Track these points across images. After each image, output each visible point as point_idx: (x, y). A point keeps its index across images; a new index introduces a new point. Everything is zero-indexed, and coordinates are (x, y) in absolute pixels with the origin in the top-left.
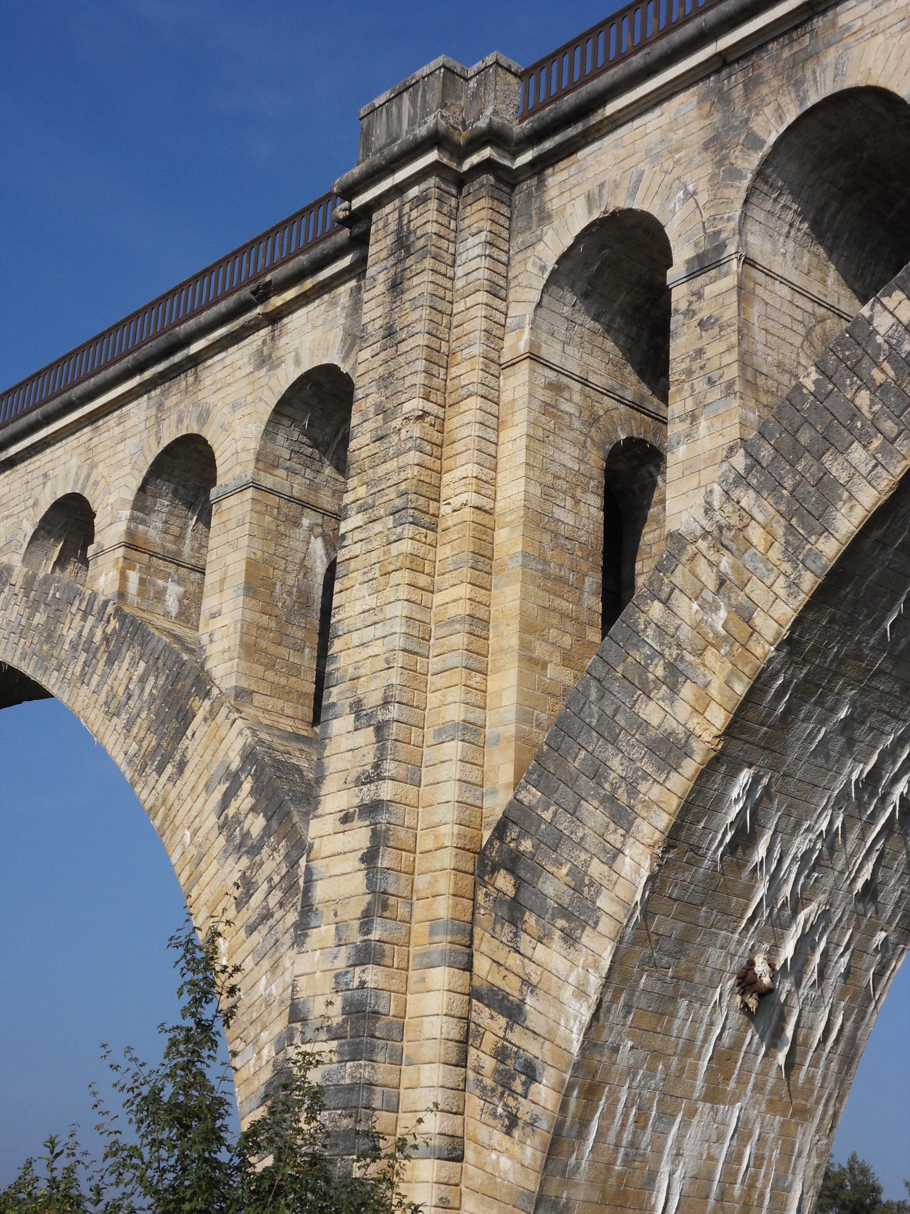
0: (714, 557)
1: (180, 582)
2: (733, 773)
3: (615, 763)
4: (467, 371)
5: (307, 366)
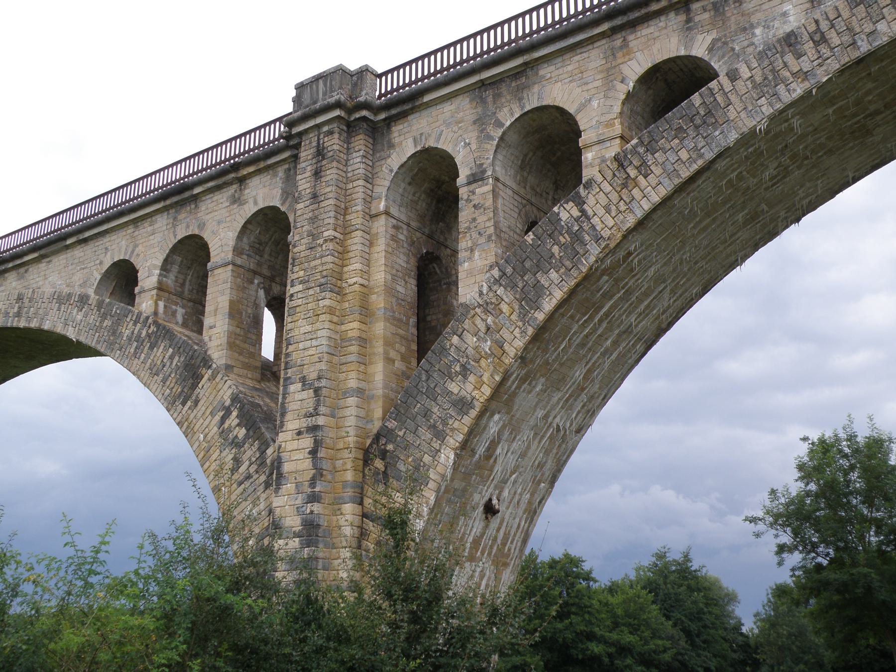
0: (484, 317)
1: (183, 307)
2: (492, 415)
3: (435, 410)
4: (356, 219)
5: (261, 205)
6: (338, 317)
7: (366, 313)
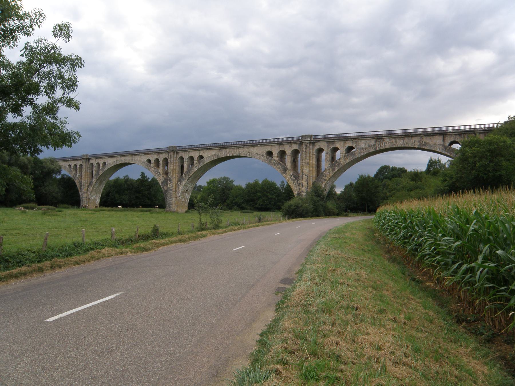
4: (311, 155)
6: (310, 167)
7: (313, 167)
